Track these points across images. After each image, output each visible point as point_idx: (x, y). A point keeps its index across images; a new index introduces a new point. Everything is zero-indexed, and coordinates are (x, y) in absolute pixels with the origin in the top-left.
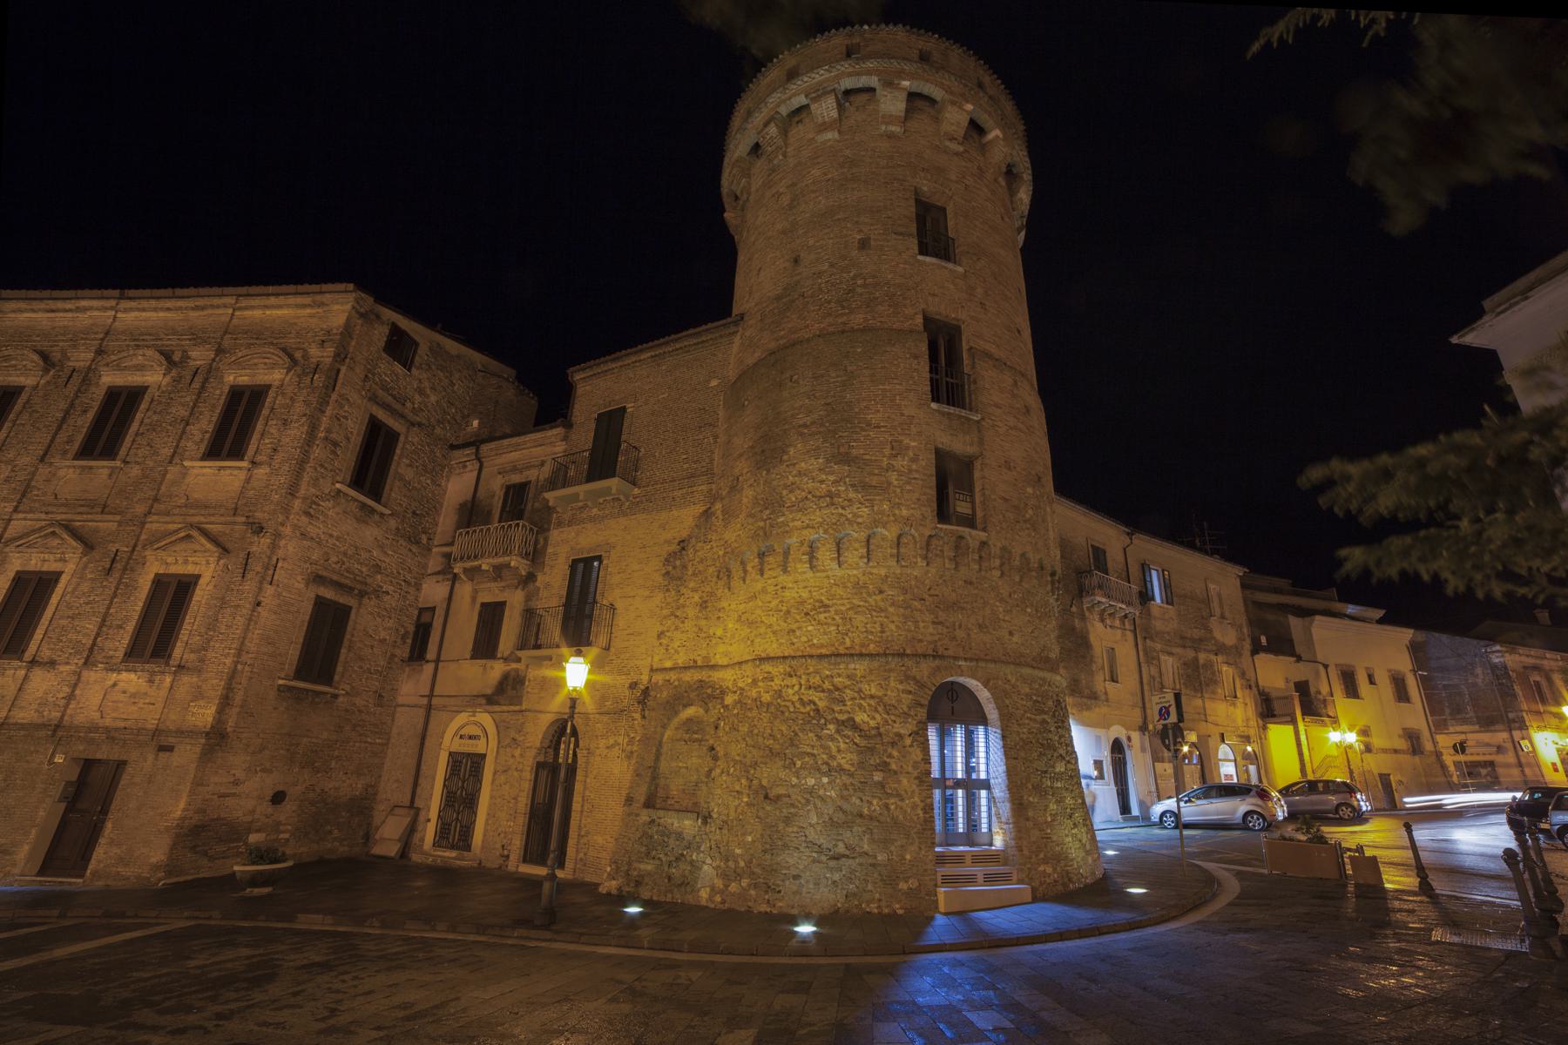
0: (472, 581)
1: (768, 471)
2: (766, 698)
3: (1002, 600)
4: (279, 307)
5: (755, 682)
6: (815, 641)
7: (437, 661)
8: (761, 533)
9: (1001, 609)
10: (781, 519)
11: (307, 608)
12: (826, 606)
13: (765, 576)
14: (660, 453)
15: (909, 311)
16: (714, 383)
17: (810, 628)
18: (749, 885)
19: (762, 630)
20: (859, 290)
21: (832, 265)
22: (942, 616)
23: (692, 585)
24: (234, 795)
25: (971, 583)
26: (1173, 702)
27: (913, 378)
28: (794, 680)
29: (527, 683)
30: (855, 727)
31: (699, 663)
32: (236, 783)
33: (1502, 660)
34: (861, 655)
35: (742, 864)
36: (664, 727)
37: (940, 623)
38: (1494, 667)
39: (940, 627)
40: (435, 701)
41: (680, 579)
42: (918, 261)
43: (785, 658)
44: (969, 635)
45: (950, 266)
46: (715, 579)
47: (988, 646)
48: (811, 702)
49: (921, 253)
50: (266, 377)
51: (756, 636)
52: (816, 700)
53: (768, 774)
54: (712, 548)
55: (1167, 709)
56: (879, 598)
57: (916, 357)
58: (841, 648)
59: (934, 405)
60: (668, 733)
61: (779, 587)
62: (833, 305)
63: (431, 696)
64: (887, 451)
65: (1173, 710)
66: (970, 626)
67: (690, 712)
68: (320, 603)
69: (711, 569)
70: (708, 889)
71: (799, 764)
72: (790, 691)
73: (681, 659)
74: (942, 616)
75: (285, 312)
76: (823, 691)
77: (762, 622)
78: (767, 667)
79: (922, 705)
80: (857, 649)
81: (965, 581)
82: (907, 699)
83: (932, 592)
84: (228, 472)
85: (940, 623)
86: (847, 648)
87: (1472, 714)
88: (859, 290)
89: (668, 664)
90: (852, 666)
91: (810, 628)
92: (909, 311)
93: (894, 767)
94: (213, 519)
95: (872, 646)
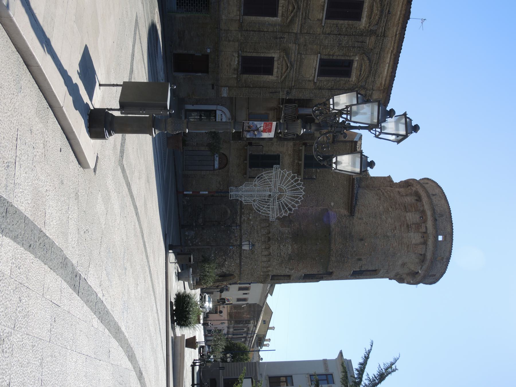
1: (291, 238)
4: (388, 70)
5: (235, 237)
8: (274, 237)
10: (276, 243)
12: (253, 254)
14: (312, 186)
16: (332, 204)
19: (248, 237)
20: (343, 259)
21: (354, 251)
26: (230, 303)
29: (239, 141)
30: (225, 261)
31: (243, 210)
33: (252, 323)
35: (194, 243)
38: (249, 321)
48: (230, 252)
50: (354, 74)
51: (247, 235)
52: (231, 253)
55: (229, 301)
56: (254, 264)
58: (243, 257)
59: (303, 275)
61: (259, 242)
62: (340, 252)
64: (291, 267)
65: (228, 303)
67: (229, 212)
70: (188, 234)
75: (385, 73)
76: (233, 255)
77: (251, 237)
78: (239, 240)
79: (229, 272)
80: (242, 260)
82: (231, 270)
84: (314, 72)
86: (242, 258)
87: (234, 311)
88: (343, 259)
90: (238, 260)
94: (294, 72)
95: (243, 264)
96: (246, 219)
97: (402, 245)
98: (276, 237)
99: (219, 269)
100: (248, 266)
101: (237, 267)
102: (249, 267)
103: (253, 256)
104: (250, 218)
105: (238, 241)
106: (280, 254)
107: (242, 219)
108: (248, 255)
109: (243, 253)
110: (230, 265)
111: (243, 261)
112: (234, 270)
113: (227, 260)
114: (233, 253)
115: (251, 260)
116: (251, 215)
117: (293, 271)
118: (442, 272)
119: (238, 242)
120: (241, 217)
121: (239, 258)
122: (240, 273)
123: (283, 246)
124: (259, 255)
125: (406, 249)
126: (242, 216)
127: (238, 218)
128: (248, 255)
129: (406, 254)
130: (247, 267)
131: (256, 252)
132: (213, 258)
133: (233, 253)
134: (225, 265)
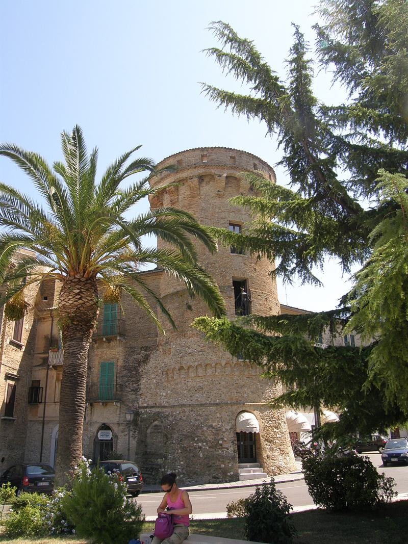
0: (56, 370)
2: (184, 418)
6: (199, 399)
7: (45, 403)
13: (181, 377)
15: (228, 278)
17: (197, 395)
18: (183, 477)
22: (239, 390)
23: (152, 376)
25: (249, 378)
27: (229, 306)
28: (193, 413)
30: (211, 426)
34: (214, 404)
36: (147, 428)
37: (239, 392)
40: (46, 419)
41: (146, 373)
42: (230, 256)
43: (190, 405)
45: (242, 255)
46: (161, 375)
49: (231, 253)
53: (185, 444)
54: (159, 363)
57: (230, 297)
60: (149, 431)
63: (44, 417)
67: (156, 423)
69: (160, 371)
71: (196, 439)
72: (192, 416)
73: (151, 403)
74: (239, 390)
82: (228, 418)
85: (239, 392)
89: (145, 405)
90: (211, 408)
91: (197, 395)
92: (228, 278)
93: (225, 439)
95: (217, 401)
96: (166, 400)
97: (191, 205)
98: (179, 359)
99: (225, 435)
100: (221, 393)
102: (224, 392)
103: (206, 389)
104: (164, 394)
105: (184, 410)
106: (199, 351)
107: (166, 405)
108: (205, 395)
109: (201, 401)
110: (218, 419)
111: (214, 401)
113: (210, 424)
114: (200, 415)
115: (213, 390)
116: (161, 394)
119: (185, 409)
120: (164, 407)
121: (208, 408)
122: (237, 403)
123: (189, 348)
124: (204, 380)
125: (196, 199)
126: (163, 405)
127: (164, 410)
128: (205, 395)
129: (202, 197)
131: (201, 385)
132: (204, 444)
133: (200, 415)
134: (219, 426)
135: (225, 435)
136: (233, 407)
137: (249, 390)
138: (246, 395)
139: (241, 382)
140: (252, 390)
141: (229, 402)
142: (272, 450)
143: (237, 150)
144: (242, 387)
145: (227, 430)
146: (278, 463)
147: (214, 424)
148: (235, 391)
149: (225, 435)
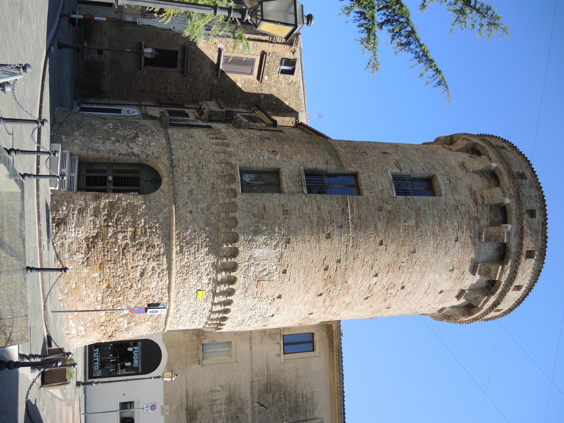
3: (208, 208)
9: (203, 206)
11: (172, 48)
22: (193, 170)
24: (101, 33)
25: (213, 188)
32: (105, 33)
39: (187, 169)
44: (185, 184)
47: (182, 196)
66: (190, 185)
68: (176, 53)
74: (193, 170)
81: (213, 184)
82: (150, 152)
83: (204, 167)
99: (123, 145)
101: (163, 149)
112: (156, 154)
117: (278, 156)
118: (527, 167)
122: (172, 166)
130: (184, 152)
135: (124, 144)
136: (167, 160)
137: (194, 187)
138: (185, 179)
139: (205, 173)
140: (195, 192)
141: (173, 157)
142: (96, 214)
143: (538, 179)
144: (198, 175)
145: (132, 148)
146: (73, 221)
147: (140, 139)
148: (191, 164)
149: (124, 144)
